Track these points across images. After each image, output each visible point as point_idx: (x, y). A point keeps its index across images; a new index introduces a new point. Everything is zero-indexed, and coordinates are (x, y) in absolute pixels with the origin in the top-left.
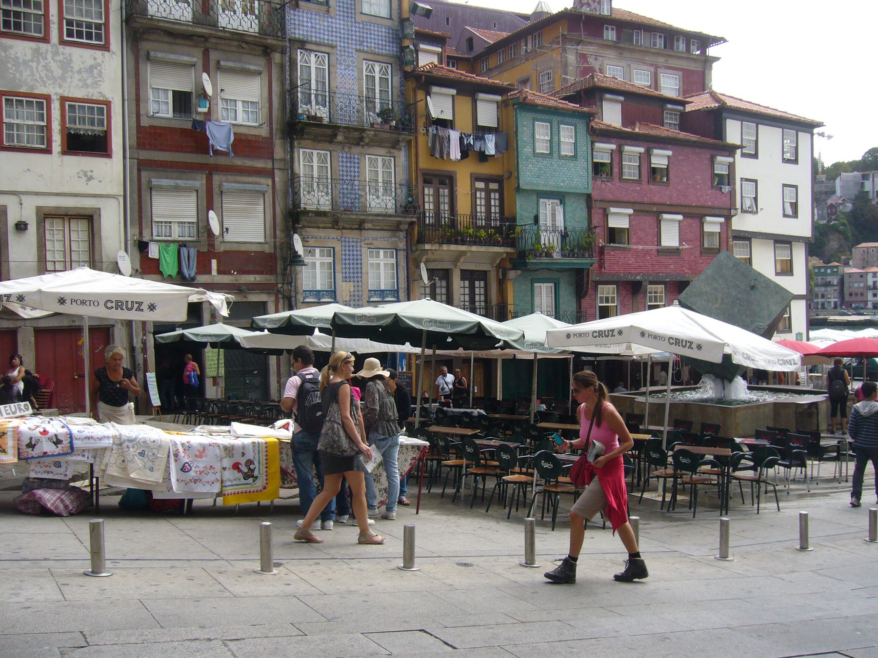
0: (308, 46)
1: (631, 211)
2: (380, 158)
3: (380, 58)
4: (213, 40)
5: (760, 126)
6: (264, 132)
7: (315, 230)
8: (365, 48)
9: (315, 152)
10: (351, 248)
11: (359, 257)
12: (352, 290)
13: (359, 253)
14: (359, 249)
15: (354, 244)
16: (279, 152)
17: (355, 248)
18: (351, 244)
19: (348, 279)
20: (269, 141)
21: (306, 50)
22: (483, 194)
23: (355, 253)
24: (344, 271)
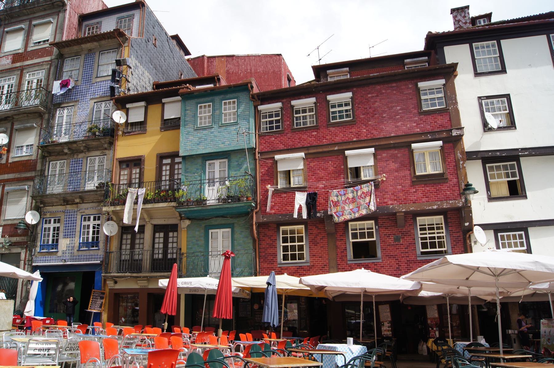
0: (63, 106)
1: (302, 154)
2: (97, 158)
3: (105, 99)
4: (15, 117)
5: (503, 42)
6: (34, 158)
7: (51, 207)
8: (96, 96)
9: (58, 162)
10: (70, 216)
11: (75, 222)
12: (68, 243)
13: (75, 219)
14: (75, 216)
15: (73, 214)
16: (39, 167)
17: (73, 216)
18: (71, 214)
19: (66, 236)
20: (36, 161)
21: (62, 107)
22: (168, 168)
23: (73, 219)
24: (65, 231)
